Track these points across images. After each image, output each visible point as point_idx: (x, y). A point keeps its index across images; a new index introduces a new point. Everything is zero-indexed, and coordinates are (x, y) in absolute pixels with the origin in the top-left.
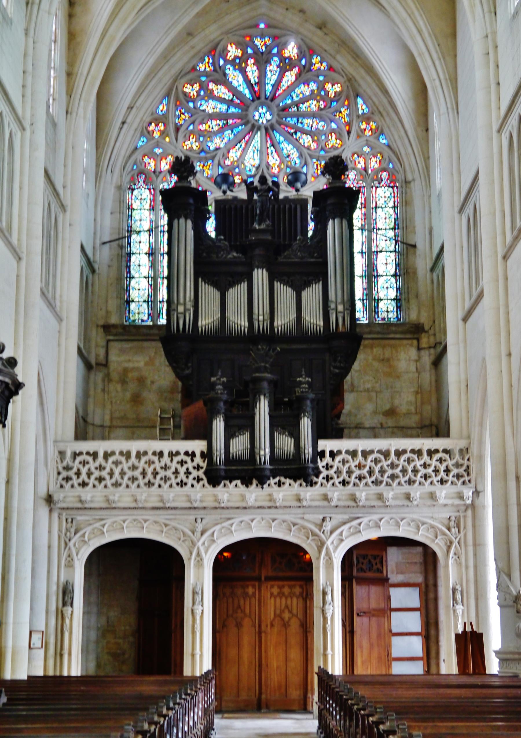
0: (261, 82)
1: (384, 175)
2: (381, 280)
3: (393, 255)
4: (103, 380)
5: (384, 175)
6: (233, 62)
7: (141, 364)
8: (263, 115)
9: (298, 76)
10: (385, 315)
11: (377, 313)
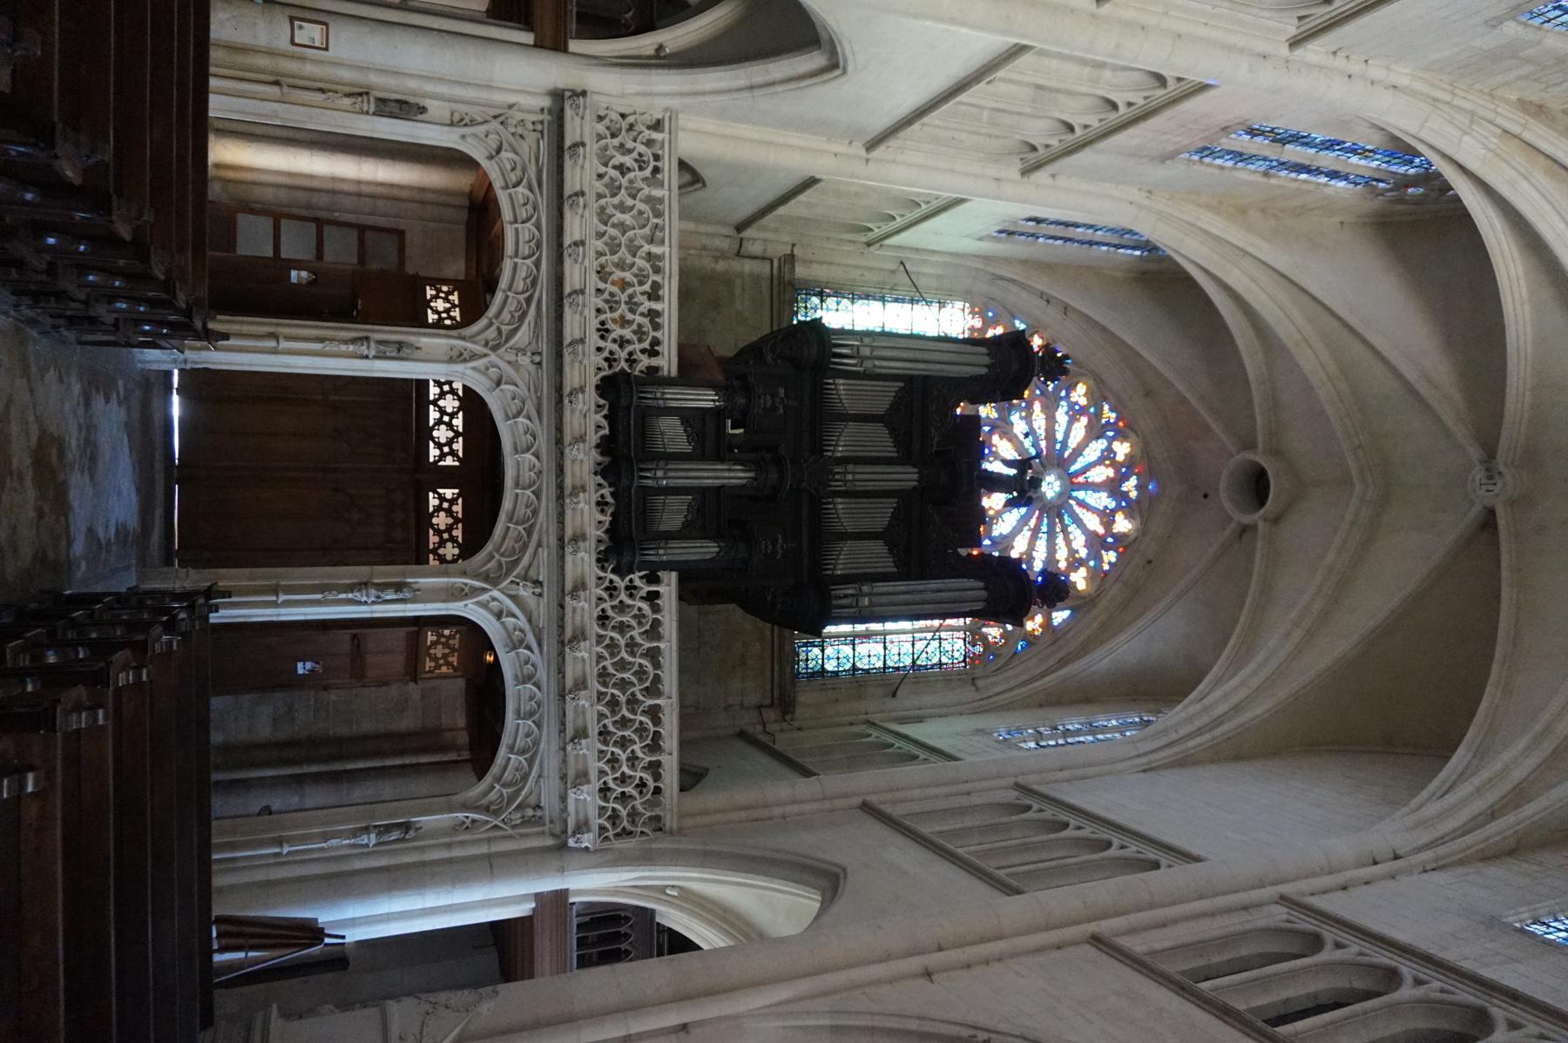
0: (1089, 486)
1: (979, 649)
2: (847, 650)
3: (880, 664)
4: (716, 250)
5: (979, 649)
6: (1109, 450)
7: (738, 306)
8: (1051, 486)
9: (1095, 534)
10: (803, 656)
11: (805, 645)
